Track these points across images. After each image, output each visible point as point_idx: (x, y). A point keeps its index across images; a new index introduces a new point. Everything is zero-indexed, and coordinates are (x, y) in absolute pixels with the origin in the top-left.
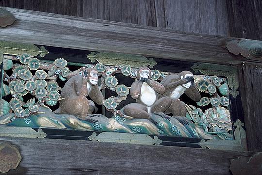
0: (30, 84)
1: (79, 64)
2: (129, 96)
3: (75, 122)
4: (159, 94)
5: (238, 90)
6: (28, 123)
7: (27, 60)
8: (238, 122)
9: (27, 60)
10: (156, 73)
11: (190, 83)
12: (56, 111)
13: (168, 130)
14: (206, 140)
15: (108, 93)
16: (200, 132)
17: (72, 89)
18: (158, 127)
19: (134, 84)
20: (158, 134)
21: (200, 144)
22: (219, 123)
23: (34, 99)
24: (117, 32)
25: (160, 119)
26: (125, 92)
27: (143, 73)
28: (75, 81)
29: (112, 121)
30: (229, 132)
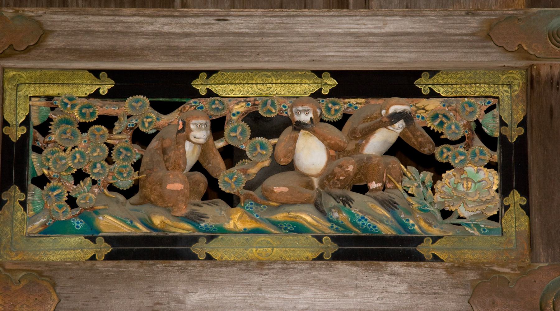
0: (78, 156)
1: (177, 100)
3: (163, 222)
6: (78, 227)
7: (73, 106)
8: (516, 197)
10: (334, 104)
12: (134, 199)
13: (350, 226)
14: (435, 239)
18: (330, 221)
24: (244, 31)
25: (333, 203)
27: (299, 112)
30: (495, 218)
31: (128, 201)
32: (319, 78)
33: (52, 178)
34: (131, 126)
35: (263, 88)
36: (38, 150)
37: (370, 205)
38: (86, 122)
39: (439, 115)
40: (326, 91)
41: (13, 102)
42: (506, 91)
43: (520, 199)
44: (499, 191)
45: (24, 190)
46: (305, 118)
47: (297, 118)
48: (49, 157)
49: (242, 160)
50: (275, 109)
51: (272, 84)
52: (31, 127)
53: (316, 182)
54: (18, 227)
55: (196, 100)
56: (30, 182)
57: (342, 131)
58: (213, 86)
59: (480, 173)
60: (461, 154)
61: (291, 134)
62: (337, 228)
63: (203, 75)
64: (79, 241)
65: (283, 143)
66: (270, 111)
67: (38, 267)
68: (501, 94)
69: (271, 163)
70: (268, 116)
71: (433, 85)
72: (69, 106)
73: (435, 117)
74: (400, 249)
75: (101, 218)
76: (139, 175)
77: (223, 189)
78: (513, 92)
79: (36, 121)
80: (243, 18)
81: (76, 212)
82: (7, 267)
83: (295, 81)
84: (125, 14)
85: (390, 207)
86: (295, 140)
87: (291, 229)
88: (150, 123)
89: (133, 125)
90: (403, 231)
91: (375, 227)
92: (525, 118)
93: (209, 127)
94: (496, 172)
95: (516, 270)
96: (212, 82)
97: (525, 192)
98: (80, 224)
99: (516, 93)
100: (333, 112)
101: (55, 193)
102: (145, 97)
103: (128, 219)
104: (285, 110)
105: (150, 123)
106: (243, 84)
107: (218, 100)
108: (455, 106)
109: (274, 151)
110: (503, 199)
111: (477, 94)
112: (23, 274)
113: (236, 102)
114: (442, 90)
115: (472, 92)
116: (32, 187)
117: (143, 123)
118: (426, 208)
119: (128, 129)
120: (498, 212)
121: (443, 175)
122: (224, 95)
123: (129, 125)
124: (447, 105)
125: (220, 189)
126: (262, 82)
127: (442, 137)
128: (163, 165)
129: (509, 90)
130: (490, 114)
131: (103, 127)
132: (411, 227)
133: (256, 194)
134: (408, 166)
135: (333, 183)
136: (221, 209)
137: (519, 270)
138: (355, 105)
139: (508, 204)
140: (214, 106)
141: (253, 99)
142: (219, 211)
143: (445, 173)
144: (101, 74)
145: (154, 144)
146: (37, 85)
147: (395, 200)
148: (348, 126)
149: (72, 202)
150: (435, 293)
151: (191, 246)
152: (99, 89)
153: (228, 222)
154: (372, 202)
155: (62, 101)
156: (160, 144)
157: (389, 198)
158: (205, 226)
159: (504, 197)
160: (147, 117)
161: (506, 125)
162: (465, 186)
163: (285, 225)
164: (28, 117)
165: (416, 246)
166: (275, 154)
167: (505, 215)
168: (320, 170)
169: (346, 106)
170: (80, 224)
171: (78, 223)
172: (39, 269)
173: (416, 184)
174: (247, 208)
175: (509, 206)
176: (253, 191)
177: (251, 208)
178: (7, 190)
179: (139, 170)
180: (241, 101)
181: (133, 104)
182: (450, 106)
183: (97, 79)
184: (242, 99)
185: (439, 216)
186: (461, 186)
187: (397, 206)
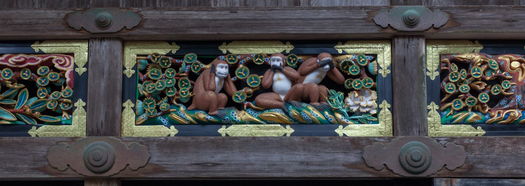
2: (261, 85)
4: (294, 81)
8: (385, 105)
9: (158, 59)
10: (293, 57)
11: (327, 67)
15: (240, 84)
19: (268, 72)
23: (166, 98)
26: (257, 82)
30: (375, 116)
36: (141, 82)
38: (165, 68)
39: (347, 63)
40: (288, 51)
45: (134, 102)
46: (278, 64)
47: (272, 63)
49: (245, 88)
50: (262, 60)
52: (138, 70)
53: (283, 97)
57: (298, 71)
60: (358, 82)
63: (224, 44)
67: (139, 140)
72: (156, 59)
73: (345, 63)
79: (140, 67)
80: (243, 11)
81: (159, 114)
82: (124, 140)
84: (183, 10)
89: (188, 70)
92: (391, 64)
95: (387, 140)
101: (150, 103)
109: (261, 81)
112: (131, 143)
116: (138, 100)
117: (194, 67)
121: (349, 94)
125: (233, 100)
134: (330, 90)
137: (388, 140)
143: (350, 93)
144: (172, 43)
149: (158, 108)
150: (345, 153)
152: (172, 50)
160: (196, 64)
164: (136, 65)
172: (140, 141)
179: (192, 92)
181: (188, 57)
183: (170, 45)
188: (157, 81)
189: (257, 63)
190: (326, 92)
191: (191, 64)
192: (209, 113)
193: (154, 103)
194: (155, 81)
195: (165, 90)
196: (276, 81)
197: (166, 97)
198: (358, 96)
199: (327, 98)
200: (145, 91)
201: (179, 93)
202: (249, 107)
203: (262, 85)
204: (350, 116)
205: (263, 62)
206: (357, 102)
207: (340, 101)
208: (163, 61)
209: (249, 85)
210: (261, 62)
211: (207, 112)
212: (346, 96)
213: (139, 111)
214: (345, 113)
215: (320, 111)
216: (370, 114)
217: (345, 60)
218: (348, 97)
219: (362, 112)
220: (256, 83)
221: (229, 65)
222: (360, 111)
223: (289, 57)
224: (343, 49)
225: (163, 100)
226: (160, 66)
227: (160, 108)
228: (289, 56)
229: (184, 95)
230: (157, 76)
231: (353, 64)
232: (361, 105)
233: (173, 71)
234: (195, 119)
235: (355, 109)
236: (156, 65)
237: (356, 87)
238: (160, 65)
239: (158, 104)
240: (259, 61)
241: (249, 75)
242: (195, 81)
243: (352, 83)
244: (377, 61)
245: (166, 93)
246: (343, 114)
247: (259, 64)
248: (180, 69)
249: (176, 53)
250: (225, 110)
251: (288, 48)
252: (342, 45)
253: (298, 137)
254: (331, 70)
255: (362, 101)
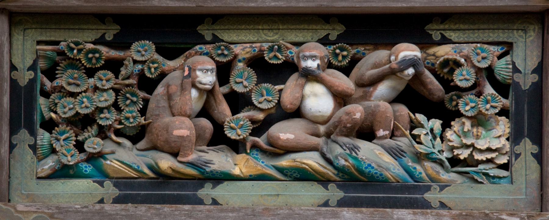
5: (534, 72)
6: (86, 171)
7: (80, 51)
9: (80, 51)
10: (342, 50)
16: (430, 172)
17: (164, 103)
18: (335, 168)
19: (293, 80)
20: (338, 179)
21: (427, 196)
22: (475, 148)
23: (95, 127)
26: (271, 98)
28: (168, 86)
29: (241, 157)
30: (505, 167)
31: (134, 146)
32: (326, 24)
33: (60, 123)
34: (137, 72)
35: (269, 34)
36: (46, 94)
37: (377, 152)
39: (450, 62)
40: (332, 37)
41: (20, 47)
42: (520, 36)
43: (532, 147)
44: (510, 139)
45: (33, 133)
48: (56, 101)
49: (248, 107)
50: (282, 55)
51: (279, 29)
53: (322, 129)
54: (28, 170)
55: (203, 46)
56: (38, 126)
58: (219, 31)
59: (490, 122)
60: (472, 101)
61: (297, 80)
62: (343, 176)
64: (88, 185)
65: (289, 90)
66: (276, 57)
68: (515, 40)
69: (276, 110)
70: (274, 62)
71: (444, 30)
72: (75, 51)
73: (446, 63)
74: (406, 198)
75: (108, 162)
76: (145, 121)
77: (229, 135)
78: (528, 38)
83: (302, 27)
85: (397, 155)
86: (303, 87)
87: (297, 176)
88: (156, 69)
89: (138, 71)
90: (409, 179)
91: (381, 175)
93: (214, 73)
94: (507, 120)
96: (218, 28)
97: (538, 140)
98: (88, 168)
99: (531, 38)
100: (340, 58)
101: (63, 137)
102: (151, 42)
103: (135, 164)
104: (292, 56)
105: (156, 69)
106: (249, 29)
107: (223, 46)
108: (467, 52)
109: (280, 97)
110: (514, 147)
111: (490, 40)
113: (241, 48)
114: (454, 36)
115: (485, 37)
116: (41, 131)
117: (150, 68)
118: (434, 156)
119: (134, 75)
120: (508, 161)
121: (453, 123)
122: (230, 40)
123: (135, 71)
124: (458, 51)
125: (226, 135)
126: (268, 28)
127: (452, 84)
128: (168, 112)
129: (524, 35)
130: (503, 60)
131: (109, 72)
132: (418, 175)
133: (261, 141)
135: (340, 130)
136: (227, 156)
138: (363, 52)
139: (519, 153)
140: (220, 52)
141: (258, 45)
142: (225, 157)
143: (454, 120)
145: (160, 89)
146: (43, 30)
147: (402, 148)
148: (355, 72)
149: (80, 146)
151: (197, 192)
153: (234, 169)
154: (379, 150)
155: (68, 46)
156: (166, 90)
157: (397, 146)
158: (211, 172)
159: (515, 145)
160: (153, 62)
161: (520, 72)
162: (475, 133)
163: (291, 172)
164: (35, 62)
165: (423, 195)
166: (281, 100)
167: (516, 163)
168: (327, 117)
169: (354, 51)
170: (88, 168)
171: (86, 167)
173: (425, 132)
174: (253, 154)
175: (520, 155)
176: (259, 137)
177: (257, 155)
178: (17, 134)
179: (145, 115)
180: (247, 47)
181: (139, 49)
182: (462, 52)
184: (248, 45)
185: (447, 163)
186: (471, 133)
187: (405, 155)
188: (78, 96)
189: (272, 62)
190: (407, 120)
191: (143, 62)
192: (179, 158)
193: (72, 137)
194: (73, 95)
195: (93, 113)
196: (309, 97)
197: (95, 125)
198: (470, 128)
199: (408, 132)
200: (56, 113)
201: (122, 118)
202: (255, 146)
203: (282, 105)
204: (453, 166)
205: (284, 59)
206: (469, 142)
207: (435, 138)
208: (90, 55)
209: (256, 103)
210: (279, 59)
211: (175, 155)
212: (446, 126)
213: (46, 151)
214: (443, 161)
215: (394, 155)
216: (495, 163)
217: (446, 57)
218: (450, 128)
219: (477, 160)
220: (270, 101)
221: (217, 62)
222: (473, 156)
223: (335, 49)
224: (442, 32)
225: (88, 131)
226: (83, 64)
227: (85, 146)
228: (334, 48)
229: (131, 123)
230: (78, 85)
231: (463, 65)
232: (476, 145)
233: (110, 75)
234: (151, 168)
235: (464, 154)
236: (74, 62)
237: (467, 111)
238: (83, 62)
239: (80, 138)
240: (276, 57)
241: (256, 85)
242: (151, 95)
243: (461, 102)
244: (512, 56)
245: (96, 118)
246: (440, 163)
247: (275, 62)
248: (123, 71)
249: (113, 39)
250: (208, 151)
251: (334, 29)
252: (442, 23)
253: (350, 209)
254: (417, 76)
255: (478, 137)
